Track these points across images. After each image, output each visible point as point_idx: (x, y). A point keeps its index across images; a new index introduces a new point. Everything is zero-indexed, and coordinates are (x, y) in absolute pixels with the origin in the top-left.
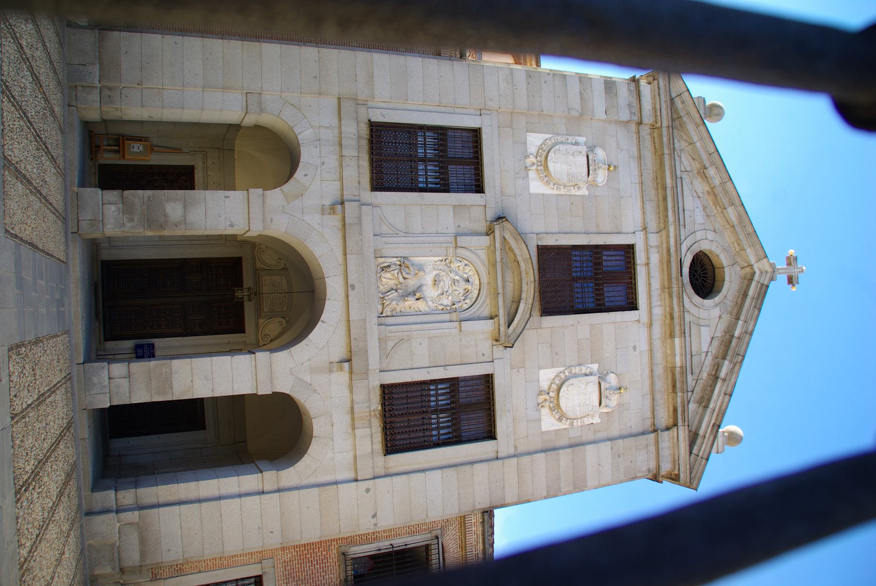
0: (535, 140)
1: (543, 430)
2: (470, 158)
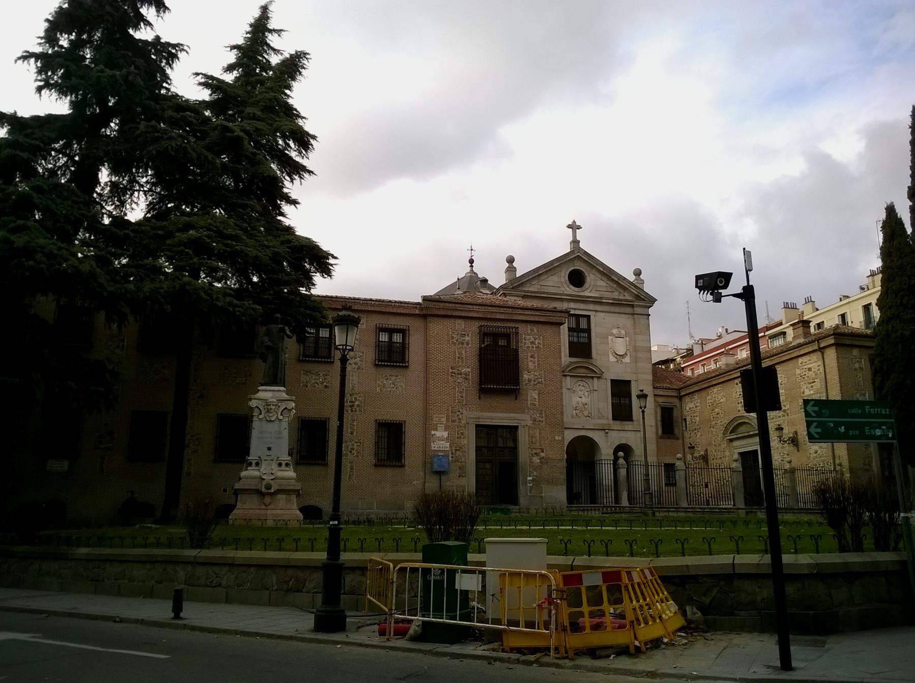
1: (629, 362)
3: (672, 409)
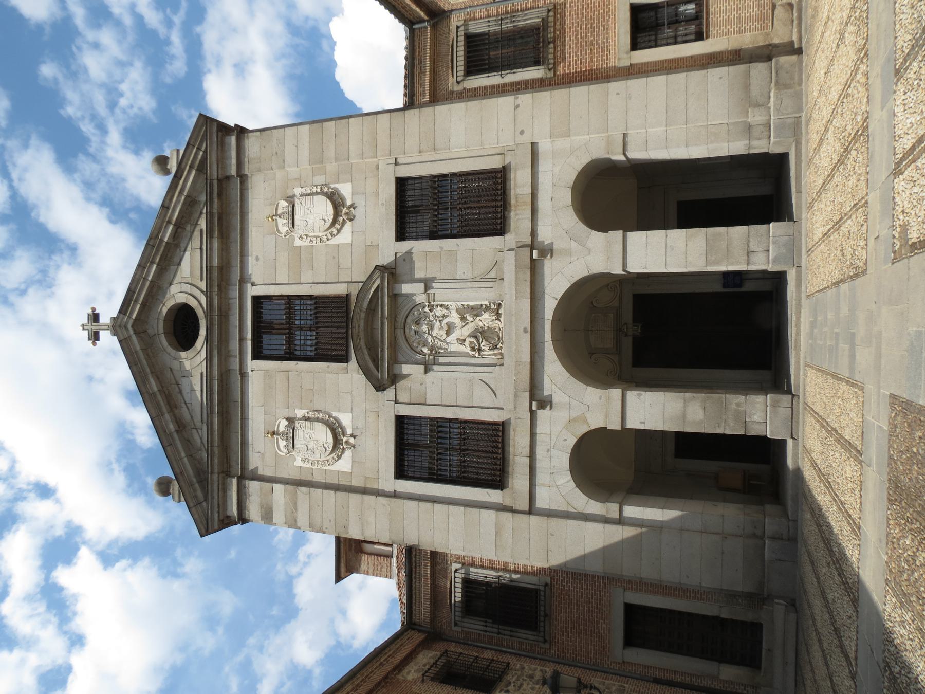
0: (345, 464)
2: (407, 450)
3: (472, 40)
